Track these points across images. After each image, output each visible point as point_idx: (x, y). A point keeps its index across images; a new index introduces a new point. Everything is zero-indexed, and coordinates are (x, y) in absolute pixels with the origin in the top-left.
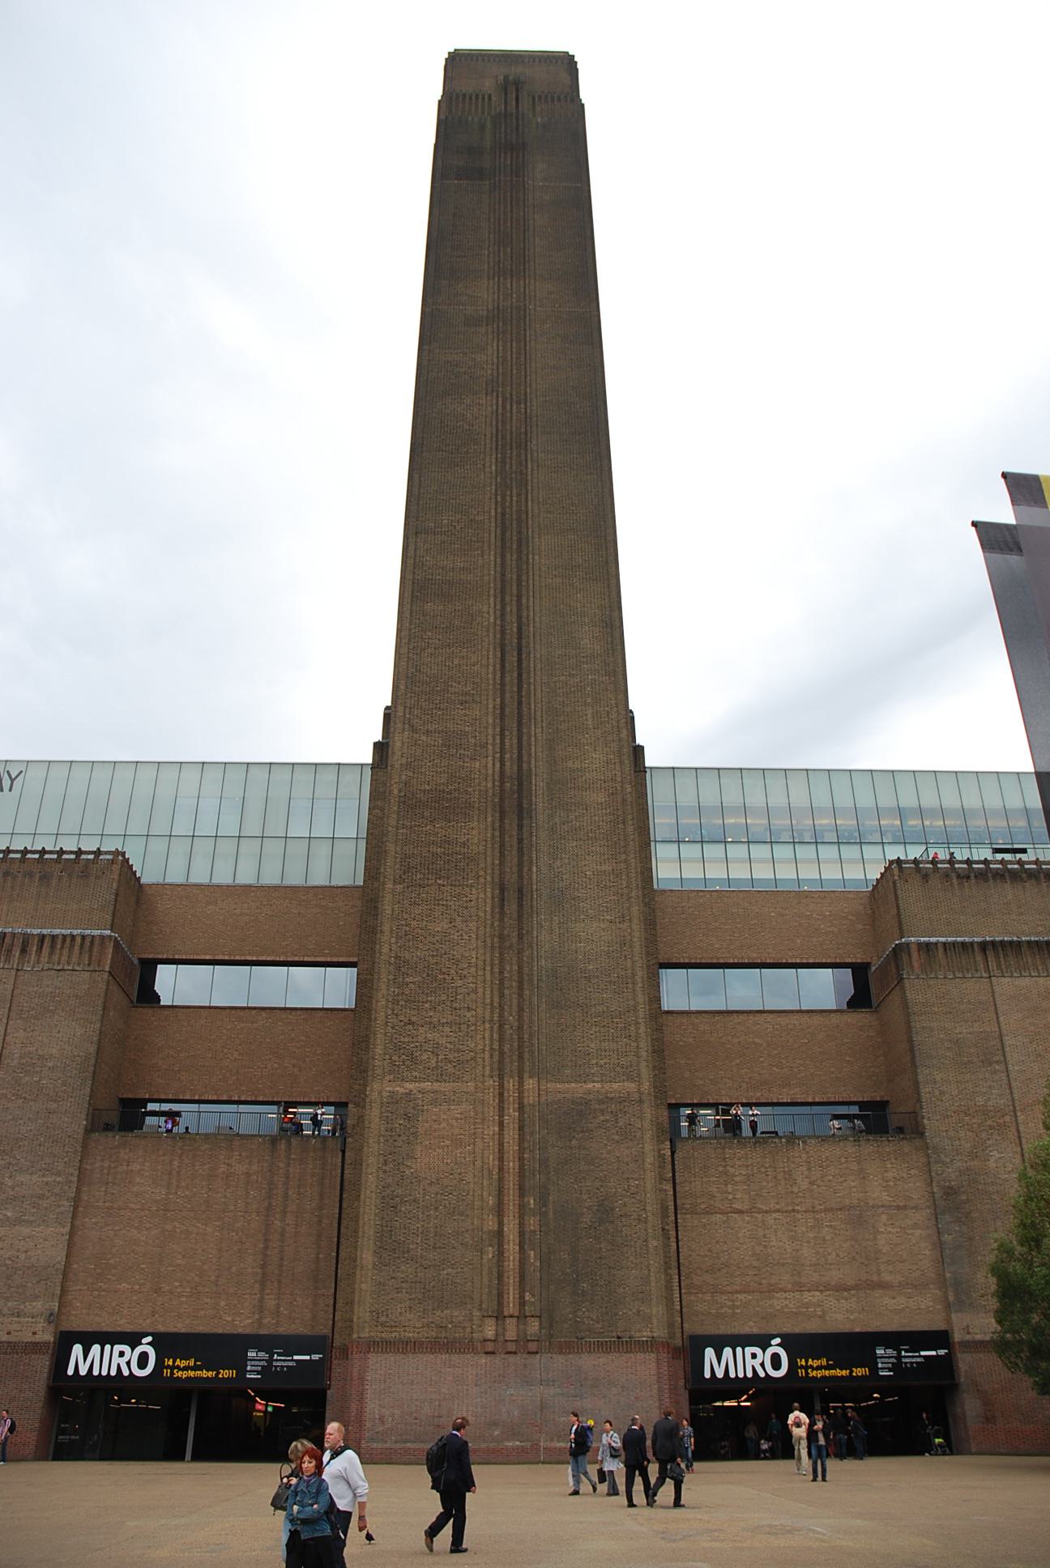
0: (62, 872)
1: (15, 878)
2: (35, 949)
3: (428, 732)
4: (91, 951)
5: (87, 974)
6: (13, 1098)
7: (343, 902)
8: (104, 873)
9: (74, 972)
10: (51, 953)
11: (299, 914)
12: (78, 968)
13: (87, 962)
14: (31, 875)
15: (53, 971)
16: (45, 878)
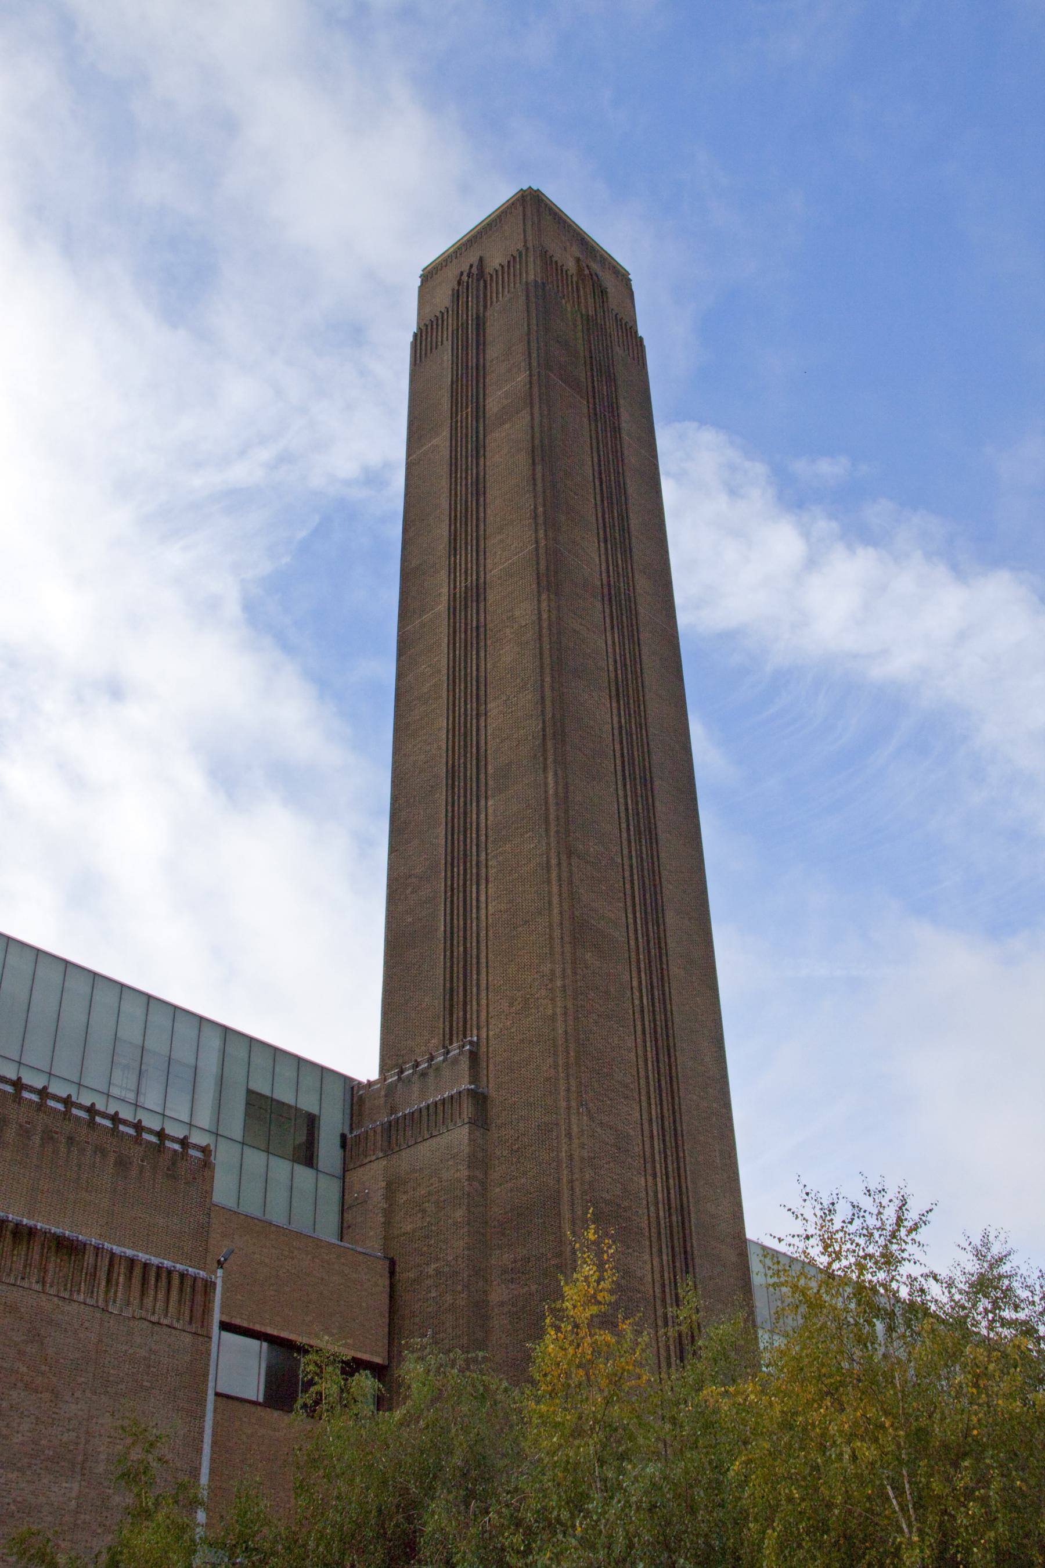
0: (142, 1161)
1: (82, 1151)
2: (121, 1279)
3: (601, 1124)
4: (193, 1301)
5: (188, 1339)
6: (99, 1531)
7: (366, 1274)
8: (194, 1178)
9: (173, 1331)
10: (143, 1293)
11: (322, 1279)
12: (176, 1325)
13: (188, 1319)
14: (100, 1150)
15: (147, 1323)
16: (122, 1164)
